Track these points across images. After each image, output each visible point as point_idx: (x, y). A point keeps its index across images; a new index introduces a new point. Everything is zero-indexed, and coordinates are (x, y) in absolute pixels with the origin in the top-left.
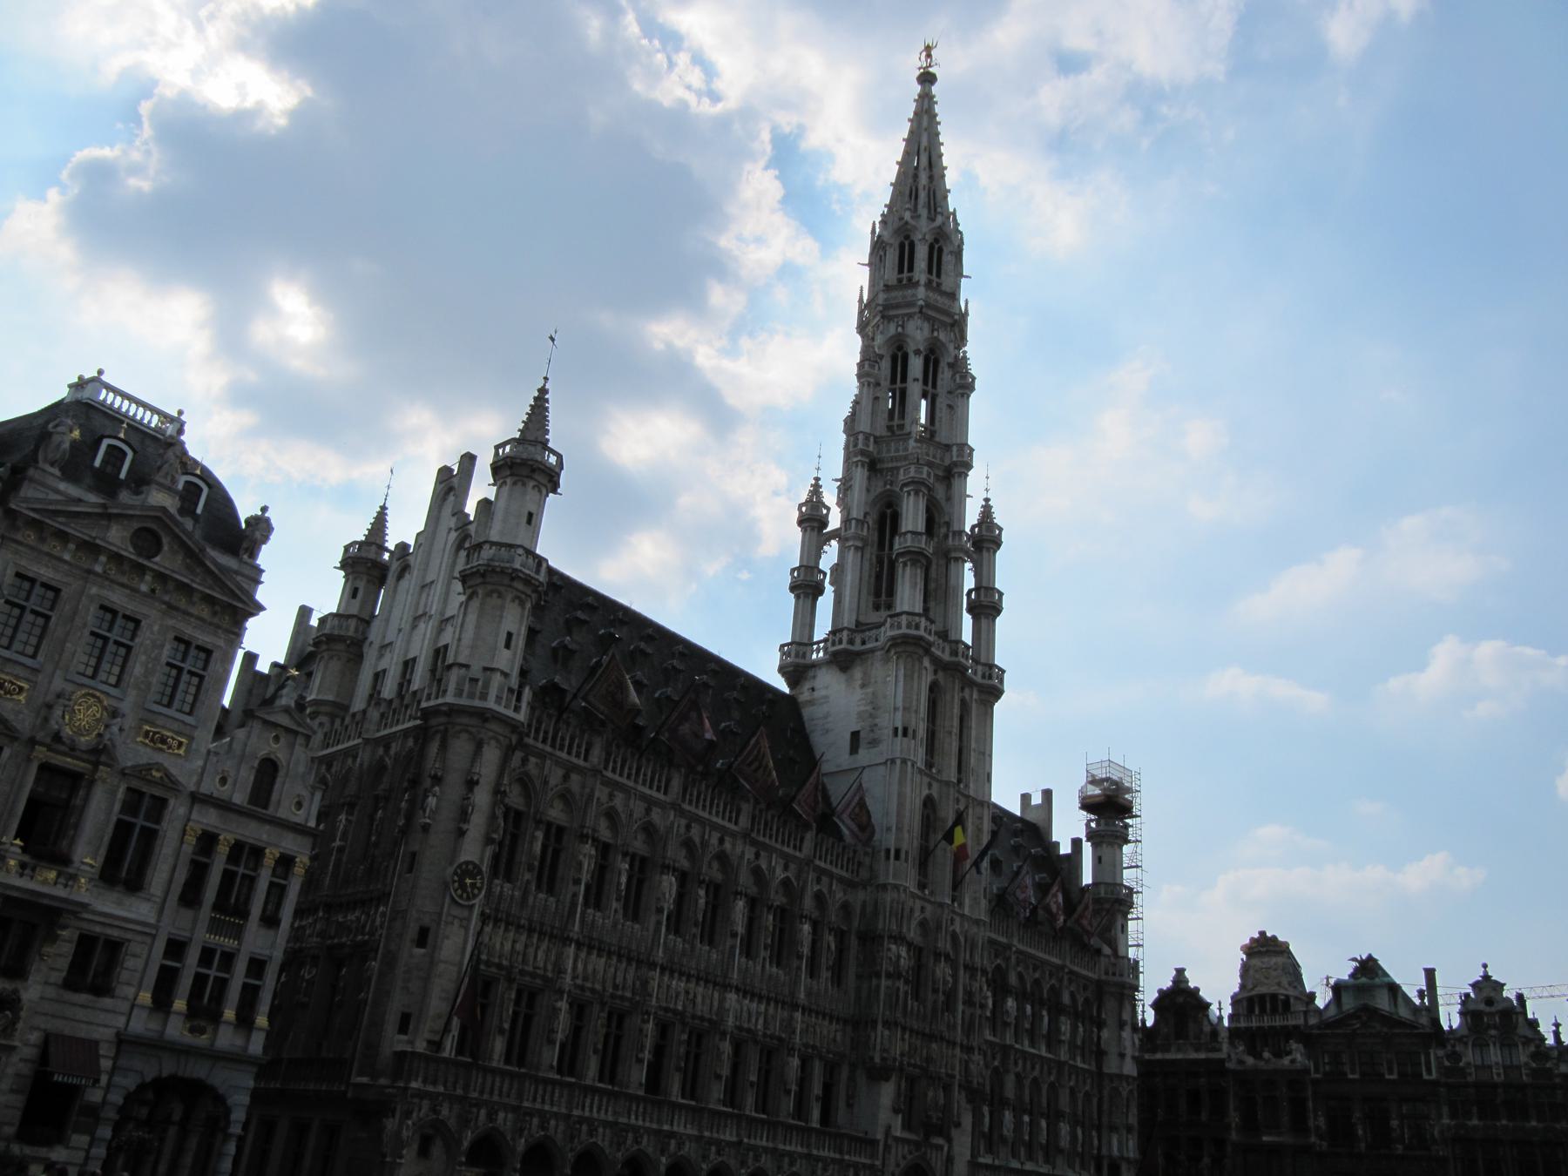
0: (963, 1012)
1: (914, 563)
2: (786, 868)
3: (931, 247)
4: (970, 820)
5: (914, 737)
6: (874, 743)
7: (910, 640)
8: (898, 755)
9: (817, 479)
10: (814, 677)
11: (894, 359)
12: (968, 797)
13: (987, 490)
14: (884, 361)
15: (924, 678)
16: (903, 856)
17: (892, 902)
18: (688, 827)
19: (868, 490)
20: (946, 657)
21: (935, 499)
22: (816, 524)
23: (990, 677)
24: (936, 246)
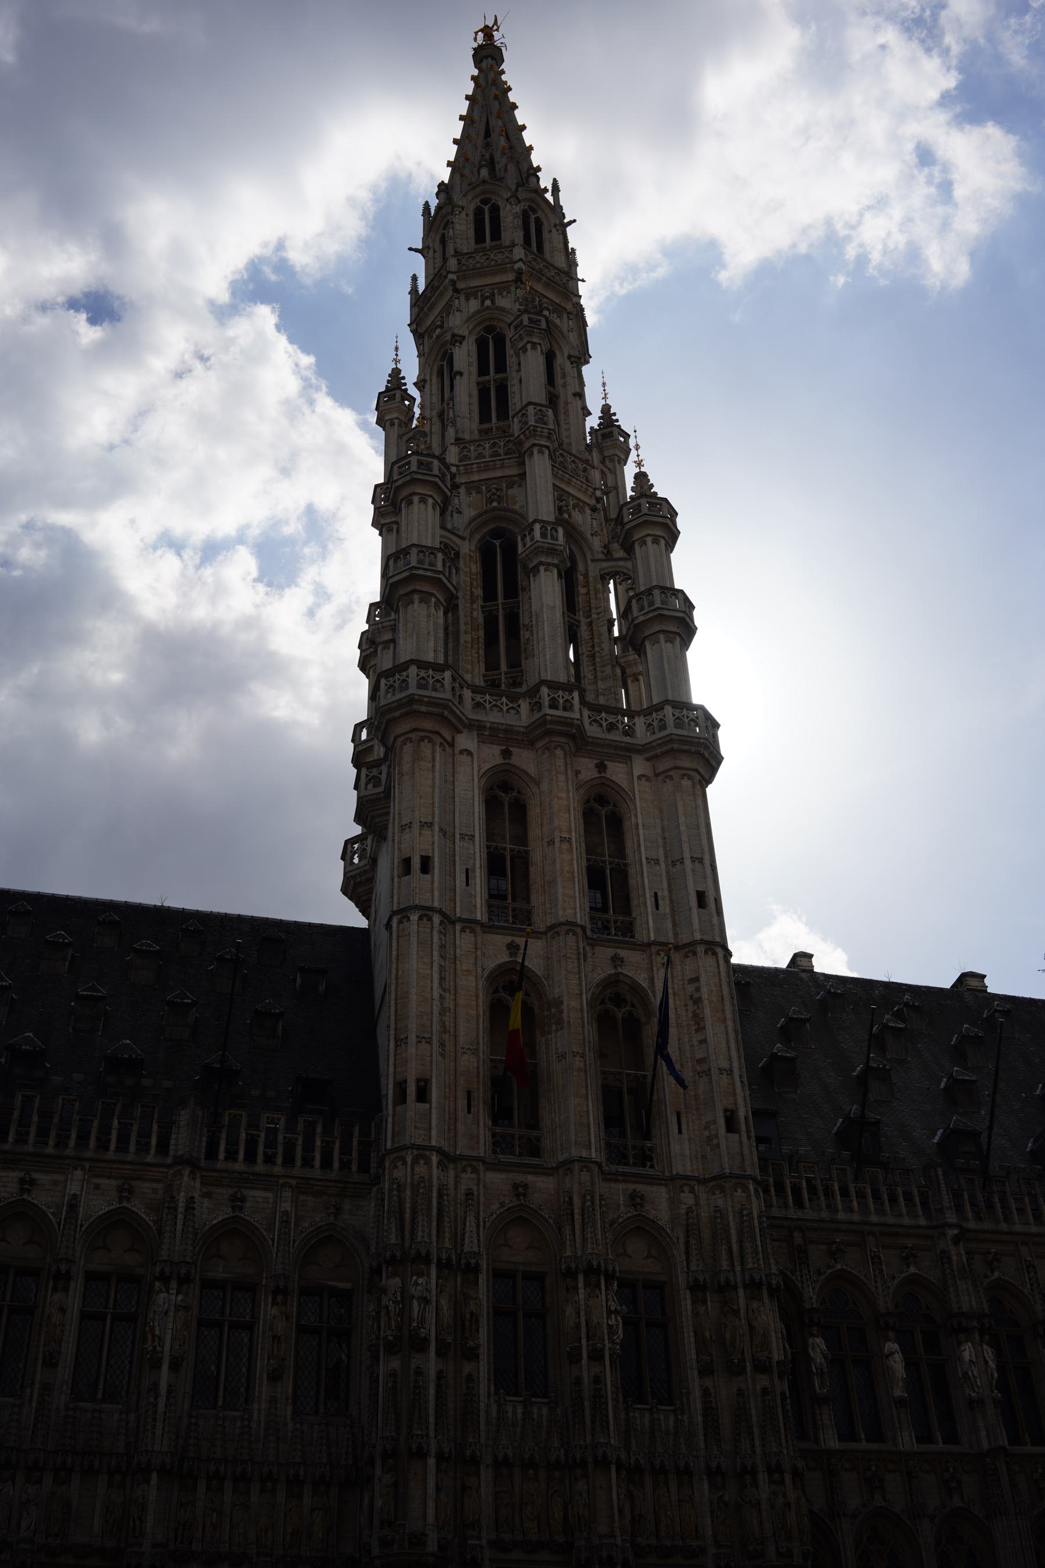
0: (706, 1393)
3: (479, 213)
7: (396, 714)
16: (412, 1090)
21: (506, 510)
23: (663, 727)
24: (486, 208)
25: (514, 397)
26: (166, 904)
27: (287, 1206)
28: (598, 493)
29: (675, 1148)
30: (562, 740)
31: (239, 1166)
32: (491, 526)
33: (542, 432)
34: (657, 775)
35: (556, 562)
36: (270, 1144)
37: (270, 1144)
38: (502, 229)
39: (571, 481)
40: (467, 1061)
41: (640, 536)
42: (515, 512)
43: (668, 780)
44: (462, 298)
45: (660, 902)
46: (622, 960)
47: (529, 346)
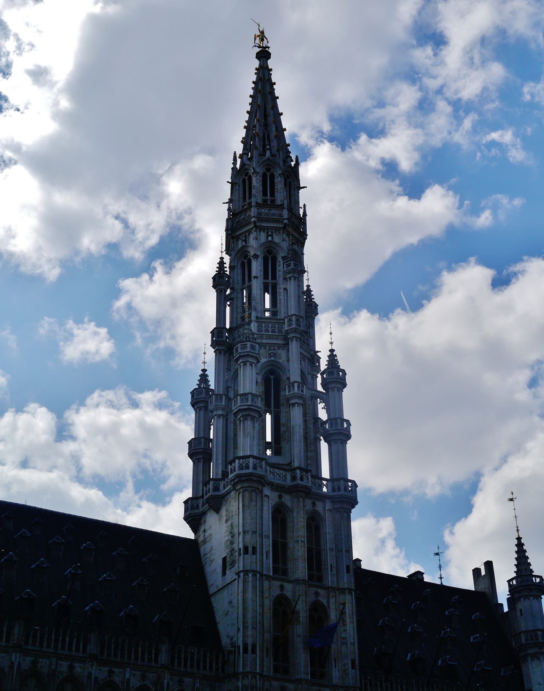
1: (245, 418)
2: (143, 677)
3: (264, 176)
4: (332, 607)
5: (254, 552)
6: (233, 563)
7: (243, 478)
8: (241, 569)
9: (204, 370)
10: (205, 521)
11: (243, 265)
12: (327, 588)
13: (331, 343)
14: (236, 270)
15: (265, 504)
16: (250, 648)
17: (242, 687)
18: (34, 663)
19: (229, 370)
20: (289, 482)
22: (202, 405)
23: (339, 490)
25: (280, 296)
26: (118, 523)
27: (197, 685)
28: (312, 353)
29: (334, 673)
30: (303, 494)
31: (182, 669)
32: (269, 368)
33: (298, 331)
34: (334, 509)
35: (301, 402)
36: (192, 660)
37: (192, 660)
38: (276, 190)
39: (302, 347)
40: (267, 636)
41: (332, 386)
42: (280, 363)
43: (338, 512)
44: (258, 231)
45: (333, 568)
46: (318, 594)
47: (292, 278)
